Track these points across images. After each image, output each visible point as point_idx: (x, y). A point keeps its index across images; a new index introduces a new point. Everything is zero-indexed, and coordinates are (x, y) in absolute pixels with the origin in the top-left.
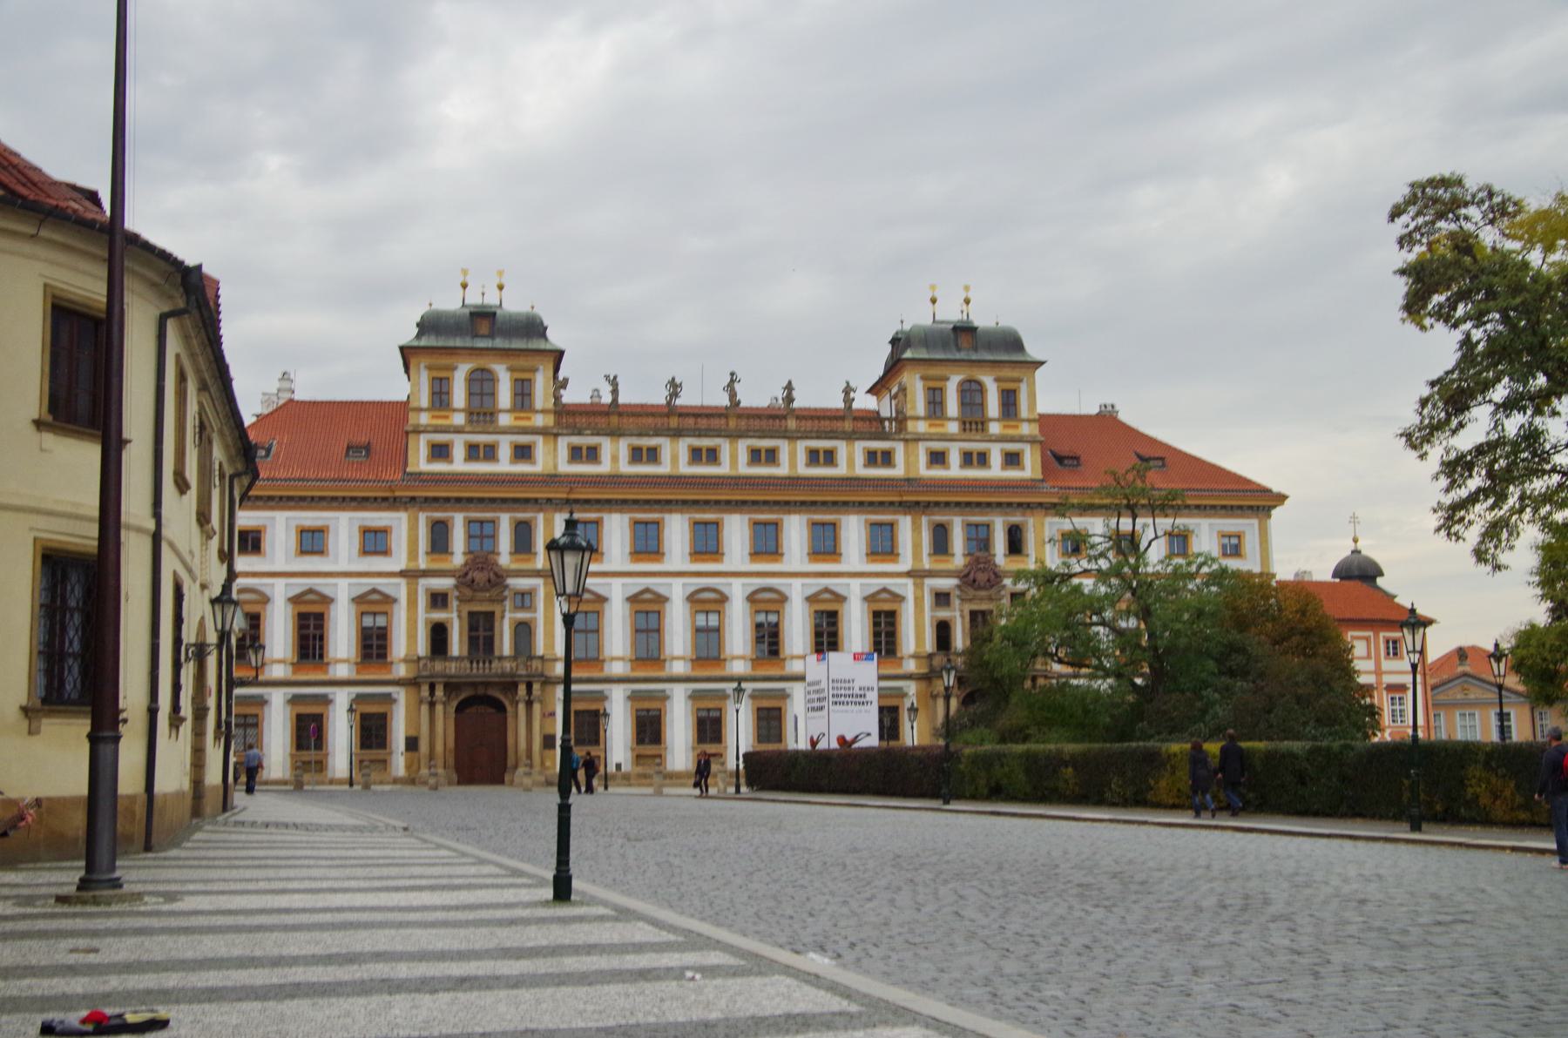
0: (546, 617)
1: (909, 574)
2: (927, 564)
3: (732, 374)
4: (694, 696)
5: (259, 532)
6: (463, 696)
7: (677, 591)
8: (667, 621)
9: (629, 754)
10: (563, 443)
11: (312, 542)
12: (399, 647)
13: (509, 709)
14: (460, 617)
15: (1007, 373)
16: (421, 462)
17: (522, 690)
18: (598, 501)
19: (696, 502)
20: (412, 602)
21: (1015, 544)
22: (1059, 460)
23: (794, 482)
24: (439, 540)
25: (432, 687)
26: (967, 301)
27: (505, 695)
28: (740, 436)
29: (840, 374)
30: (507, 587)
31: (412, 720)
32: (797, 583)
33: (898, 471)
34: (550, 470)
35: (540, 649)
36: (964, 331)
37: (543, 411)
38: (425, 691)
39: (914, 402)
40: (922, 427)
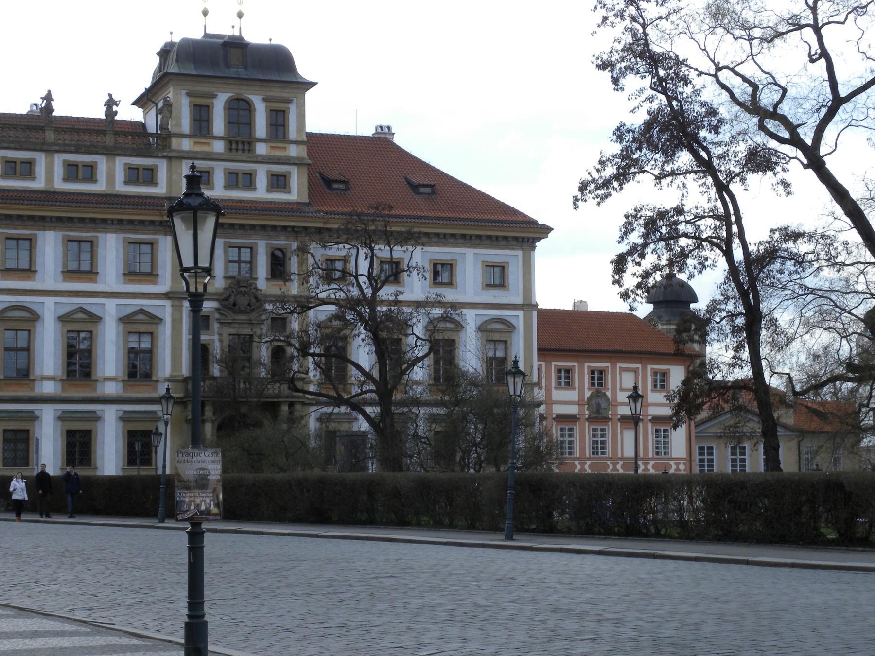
1: (167, 296)
15: (276, 92)
21: (278, 268)
22: (324, 183)
23: (49, 197)
26: (240, 15)
32: (50, 302)
39: (179, 119)
40: (186, 145)
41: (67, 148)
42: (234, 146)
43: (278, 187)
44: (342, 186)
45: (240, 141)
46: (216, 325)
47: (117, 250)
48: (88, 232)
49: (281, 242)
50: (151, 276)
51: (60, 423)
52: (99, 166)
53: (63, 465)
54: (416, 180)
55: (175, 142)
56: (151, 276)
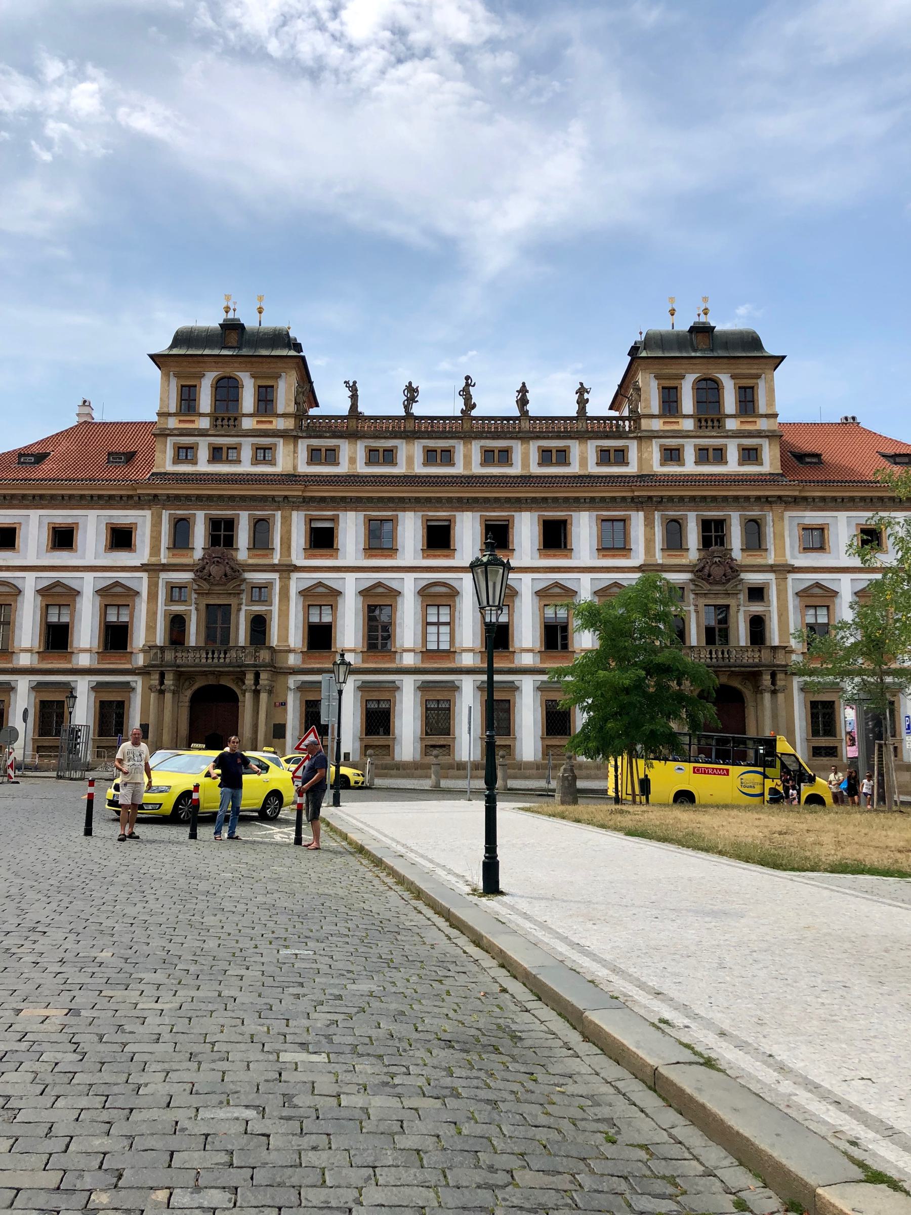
0: (280, 609)
3: (467, 378)
4: (423, 688)
5: (15, 529)
6: (196, 687)
7: (409, 585)
8: (398, 614)
9: (358, 744)
10: (303, 446)
11: (63, 538)
12: (139, 638)
13: (241, 698)
14: (197, 609)
15: (744, 369)
16: (165, 462)
17: (249, 679)
18: (333, 499)
19: (429, 500)
20: (153, 596)
23: (526, 480)
25: (162, 676)
28: (475, 438)
29: (574, 377)
30: (245, 579)
33: (632, 469)
34: (289, 469)
35: (274, 640)
36: (702, 331)
37: (284, 415)
38: (155, 680)
39: (648, 401)
40: (657, 425)
41: (542, 435)
42: (703, 423)
43: (749, 459)
44: (814, 460)
45: (709, 414)
46: (692, 596)
47: (590, 527)
48: (562, 511)
49: (754, 513)
50: (625, 550)
51: (539, 693)
52: (572, 450)
53: (543, 734)
54: (891, 452)
55: (643, 421)
56: (625, 550)
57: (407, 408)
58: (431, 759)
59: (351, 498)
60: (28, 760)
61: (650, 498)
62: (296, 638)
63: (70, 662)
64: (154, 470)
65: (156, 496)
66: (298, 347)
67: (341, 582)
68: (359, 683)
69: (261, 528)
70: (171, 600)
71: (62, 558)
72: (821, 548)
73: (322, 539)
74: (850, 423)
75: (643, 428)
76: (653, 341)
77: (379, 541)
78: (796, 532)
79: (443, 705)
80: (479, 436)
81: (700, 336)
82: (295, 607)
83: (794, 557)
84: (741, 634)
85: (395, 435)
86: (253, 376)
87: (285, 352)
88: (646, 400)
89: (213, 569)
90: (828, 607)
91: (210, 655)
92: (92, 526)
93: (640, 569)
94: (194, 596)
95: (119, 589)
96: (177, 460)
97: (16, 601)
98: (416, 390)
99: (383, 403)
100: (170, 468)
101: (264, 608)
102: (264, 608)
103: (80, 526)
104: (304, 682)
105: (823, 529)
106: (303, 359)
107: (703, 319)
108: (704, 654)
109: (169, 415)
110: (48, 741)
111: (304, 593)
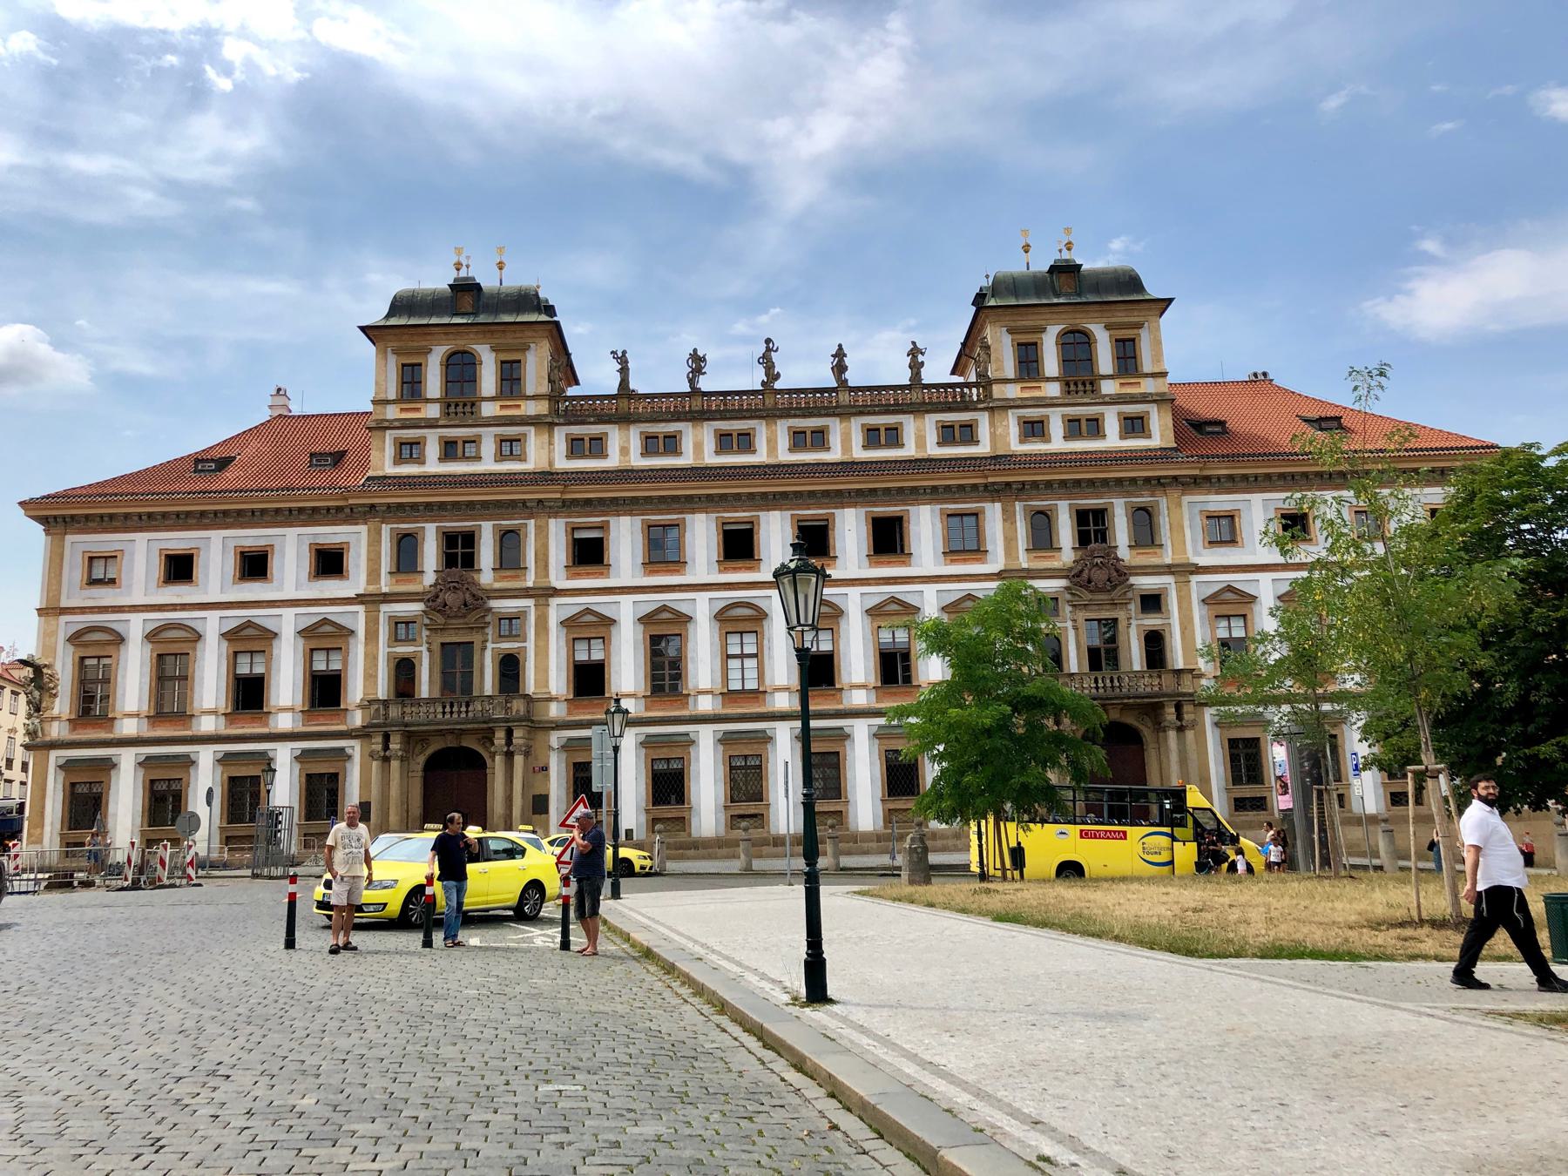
2: (1024, 561)
3: (768, 341)
4: (726, 740)
6: (430, 751)
7: (702, 608)
8: (690, 645)
9: (643, 818)
10: (560, 435)
11: (254, 565)
12: (355, 691)
13: (489, 761)
14: (429, 650)
15: (1121, 317)
16: (384, 462)
19: (723, 497)
20: (372, 635)
23: (848, 467)
24: (406, 554)
25: (387, 738)
27: (486, 749)
28: (781, 417)
29: (903, 336)
31: (365, 784)
33: (983, 448)
34: (543, 465)
35: (530, 685)
37: (534, 397)
40: (1013, 391)
42: (1072, 387)
45: (1079, 375)
46: (1068, 609)
49: (1144, 499)
54: (1315, 415)
56: (978, 551)
57: (692, 381)
58: (739, 834)
59: (624, 499)
60: (215, 855)
61: (1008, 484)
62: (558, 682)
63: (267, 725)
64: (370, 473)
65: (373, 506)
66: (550, 310)
67: (614, 607)
68: (642, 738)
69: (509, 542)
70: (395, 639)
71: (254, 590)
72: (1232, 541)
73: (589, 553)
74: (1260, 380)
75: (995, 396)
76: (1002, 286)
77: (662, 552)
78: (1199, 521)
79: (751, 762)
80: (787, 413)
81: (1063, 277)
82: (556, 642)
83: (1197, 553)
84: (1134, 655)
85: (678, 417)
86: (495, 349)
87: (533, 317)
88: (998, 360)
89: (449, 597)
90: (1244, 616)
91: (448, 709)
92: (291, 549)
93: (999, 575)
94: (425, 633)
95: (328, 628)
96: (399, 460)
97: (195, 649)
98: (703, 359)
99: (659, 375)
100: (391, 470)
101: (516, 645)
102: (516, 645)
103: (277, 548)
104: (570, 739)
105: (1232, 517)
106: (557, 324)
107: (1066, 255)
108: (1088, 683)
109: (388, 402)
110: (240, 829)
111: (568, 623)
